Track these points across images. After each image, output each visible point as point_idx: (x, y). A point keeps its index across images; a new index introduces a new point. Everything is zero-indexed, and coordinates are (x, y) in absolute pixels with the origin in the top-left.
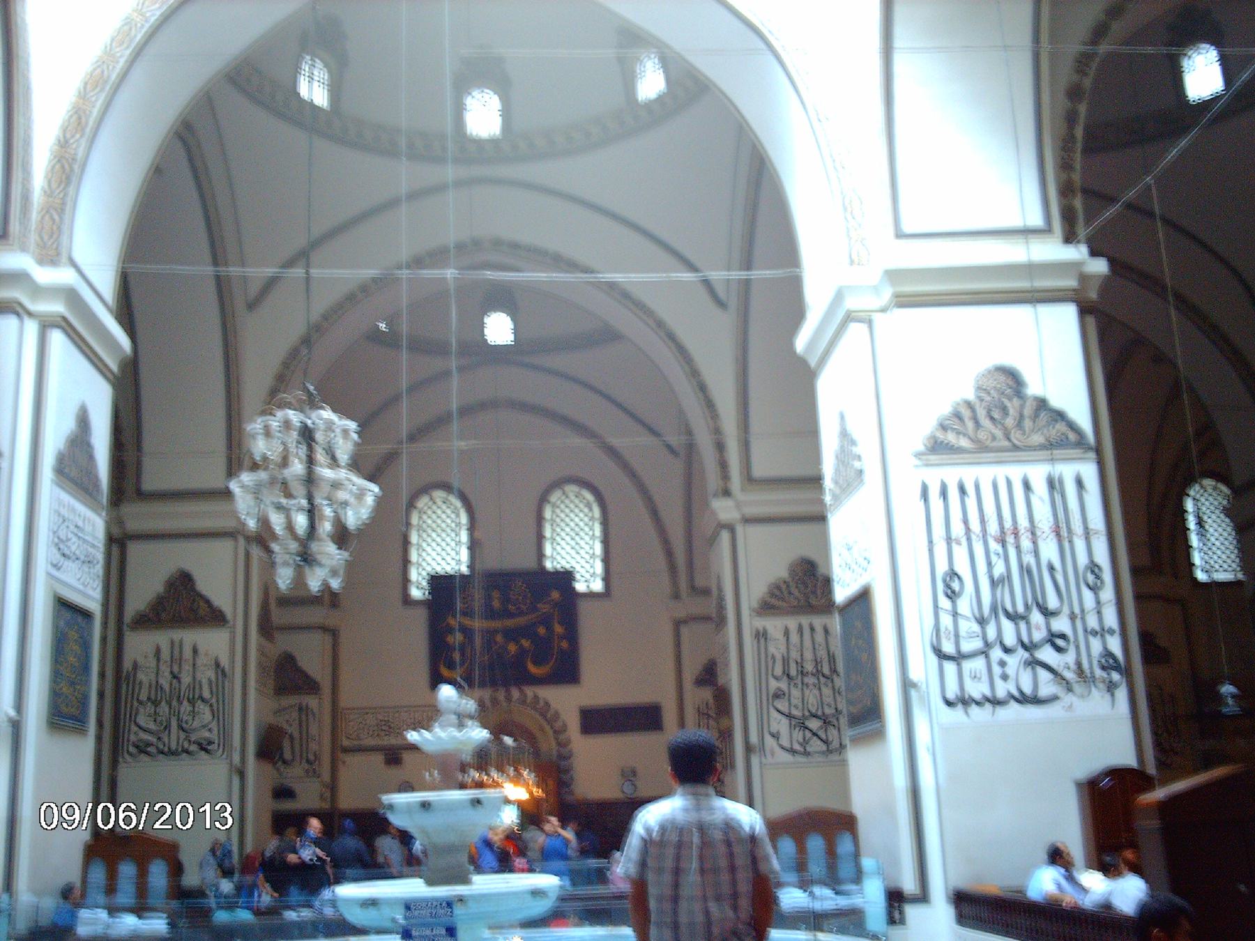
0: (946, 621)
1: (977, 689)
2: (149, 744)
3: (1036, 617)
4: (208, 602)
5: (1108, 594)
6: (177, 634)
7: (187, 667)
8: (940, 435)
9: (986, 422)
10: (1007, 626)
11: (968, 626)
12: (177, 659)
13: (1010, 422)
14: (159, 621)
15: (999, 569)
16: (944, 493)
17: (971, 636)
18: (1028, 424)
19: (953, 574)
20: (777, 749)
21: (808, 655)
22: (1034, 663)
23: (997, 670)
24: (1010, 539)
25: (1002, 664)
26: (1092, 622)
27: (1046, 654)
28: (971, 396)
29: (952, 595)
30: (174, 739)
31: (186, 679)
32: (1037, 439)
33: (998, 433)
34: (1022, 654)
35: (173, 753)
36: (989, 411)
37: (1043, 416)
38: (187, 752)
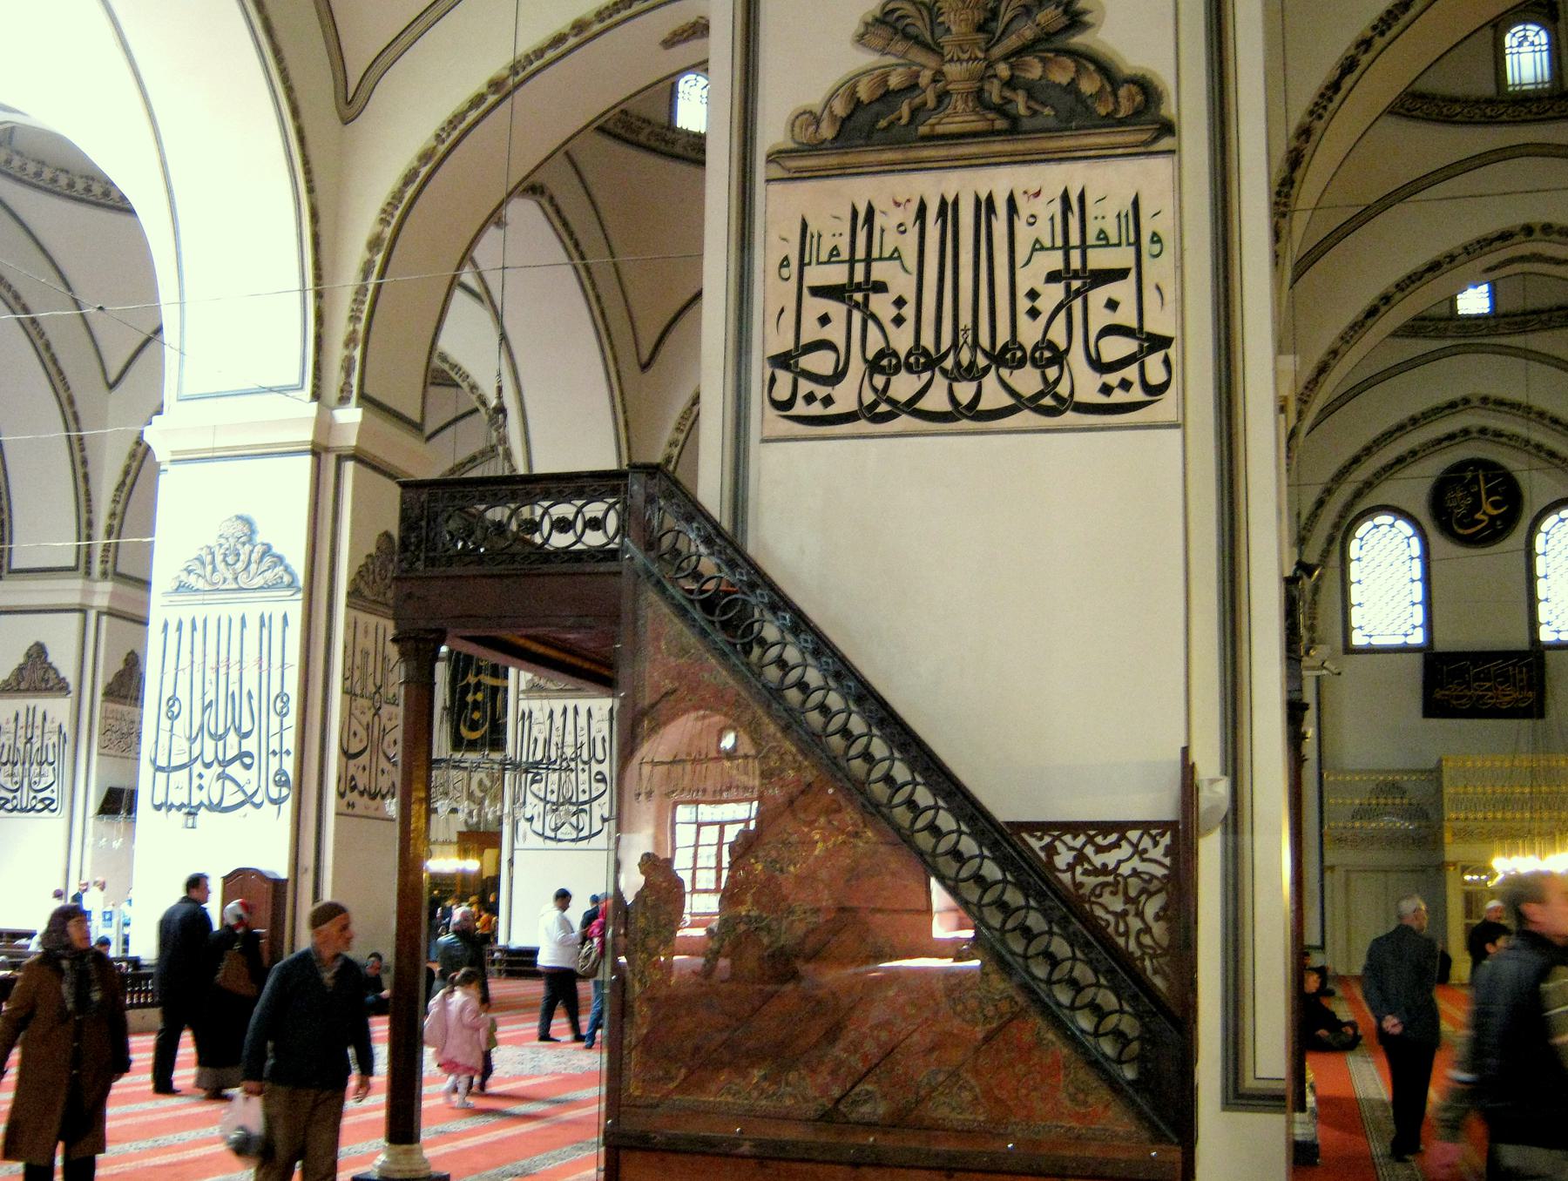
0: (164, 736)
1: (177, 798)
2: (7, 801)
3: (232, 738)
4: (56, 671)
5: (292, 720)
6: (32, 702)
7: (38, 732)
8: (184, 576)
9: (221, 566)
10: (209, 744)
11: (180, 744)
12: (30, 725)
13: (240, 566)
14: (19, 690)
15: (210, 696)
16: (179, 628)
17: (181, 752)
18: (253, 567)
19: (173, 699)
20: (530, 835)
21: (570, 739)
22: (222, 777)
23: (196, 781)
24: (223, 670)
25: (200, 776)
26: (274, 745)
27: (235, 770)
28: (213, 543)
29: (173, 718)
30: (25, 798)
31: (37, 744)
32: (258, 581)
33: (230, 576)
34: (216, 769)
35: (22, 810)
36: (225, 555)
37: (268, 560)
38: (33, 809)
